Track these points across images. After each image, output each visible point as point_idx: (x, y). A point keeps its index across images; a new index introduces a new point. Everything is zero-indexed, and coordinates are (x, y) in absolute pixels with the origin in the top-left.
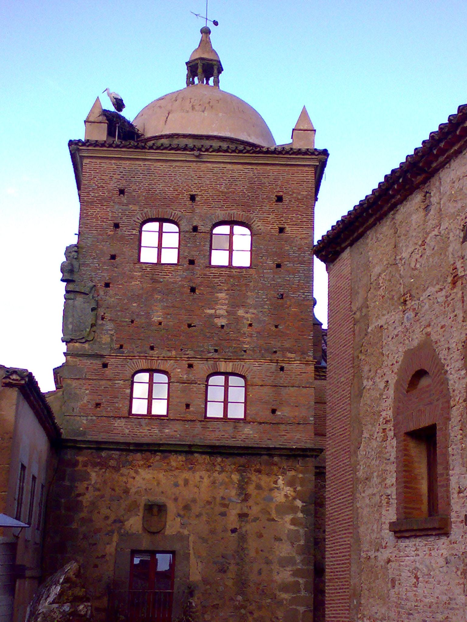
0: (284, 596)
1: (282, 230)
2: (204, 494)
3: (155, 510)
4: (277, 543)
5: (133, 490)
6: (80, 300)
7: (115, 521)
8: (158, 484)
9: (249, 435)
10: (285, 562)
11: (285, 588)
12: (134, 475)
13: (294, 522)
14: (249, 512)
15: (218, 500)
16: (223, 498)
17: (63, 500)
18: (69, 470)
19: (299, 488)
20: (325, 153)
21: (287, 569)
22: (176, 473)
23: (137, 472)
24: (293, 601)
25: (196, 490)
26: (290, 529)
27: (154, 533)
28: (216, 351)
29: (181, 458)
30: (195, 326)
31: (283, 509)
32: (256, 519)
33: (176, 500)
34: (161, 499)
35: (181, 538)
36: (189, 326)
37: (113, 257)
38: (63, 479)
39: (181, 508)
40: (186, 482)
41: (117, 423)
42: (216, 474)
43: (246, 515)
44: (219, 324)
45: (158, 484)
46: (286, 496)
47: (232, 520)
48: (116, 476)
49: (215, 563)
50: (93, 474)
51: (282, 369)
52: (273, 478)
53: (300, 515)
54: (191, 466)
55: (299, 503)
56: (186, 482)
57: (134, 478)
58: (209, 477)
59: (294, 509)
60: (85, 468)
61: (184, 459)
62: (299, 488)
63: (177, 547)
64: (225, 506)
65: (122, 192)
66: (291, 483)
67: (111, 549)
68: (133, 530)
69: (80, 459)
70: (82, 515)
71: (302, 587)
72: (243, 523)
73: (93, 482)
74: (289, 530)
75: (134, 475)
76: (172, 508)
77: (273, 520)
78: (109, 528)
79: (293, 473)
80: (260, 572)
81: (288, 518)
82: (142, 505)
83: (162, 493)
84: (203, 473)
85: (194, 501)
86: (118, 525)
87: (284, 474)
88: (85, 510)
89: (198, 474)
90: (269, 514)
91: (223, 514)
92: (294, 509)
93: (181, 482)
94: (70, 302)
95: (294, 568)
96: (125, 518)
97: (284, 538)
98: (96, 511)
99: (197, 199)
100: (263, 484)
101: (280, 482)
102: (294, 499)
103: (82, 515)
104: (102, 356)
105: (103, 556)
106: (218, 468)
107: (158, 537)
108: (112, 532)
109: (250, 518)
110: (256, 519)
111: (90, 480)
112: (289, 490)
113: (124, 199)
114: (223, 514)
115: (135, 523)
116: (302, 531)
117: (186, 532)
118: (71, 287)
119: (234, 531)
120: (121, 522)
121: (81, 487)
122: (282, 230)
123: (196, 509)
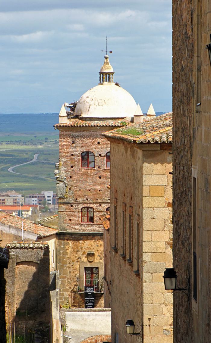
5: (84, 248)
7: (78, 258)
8: (92, 246)
17: (61, 252)
23: (85, 242)
29: (99, 237)
30: (101, 191)
33: (98, 251)
34: (92, 251)
36: (100, 191)
45: (92, 246)
50: (70, 243)
57: (83, 244)
60: (67, 241)
61: (100, 237)
75: (84, 243)
78: (77, 260)
93: (99, 245)
99: (100, 144)
105: (76, 269)
120: (80, 258)
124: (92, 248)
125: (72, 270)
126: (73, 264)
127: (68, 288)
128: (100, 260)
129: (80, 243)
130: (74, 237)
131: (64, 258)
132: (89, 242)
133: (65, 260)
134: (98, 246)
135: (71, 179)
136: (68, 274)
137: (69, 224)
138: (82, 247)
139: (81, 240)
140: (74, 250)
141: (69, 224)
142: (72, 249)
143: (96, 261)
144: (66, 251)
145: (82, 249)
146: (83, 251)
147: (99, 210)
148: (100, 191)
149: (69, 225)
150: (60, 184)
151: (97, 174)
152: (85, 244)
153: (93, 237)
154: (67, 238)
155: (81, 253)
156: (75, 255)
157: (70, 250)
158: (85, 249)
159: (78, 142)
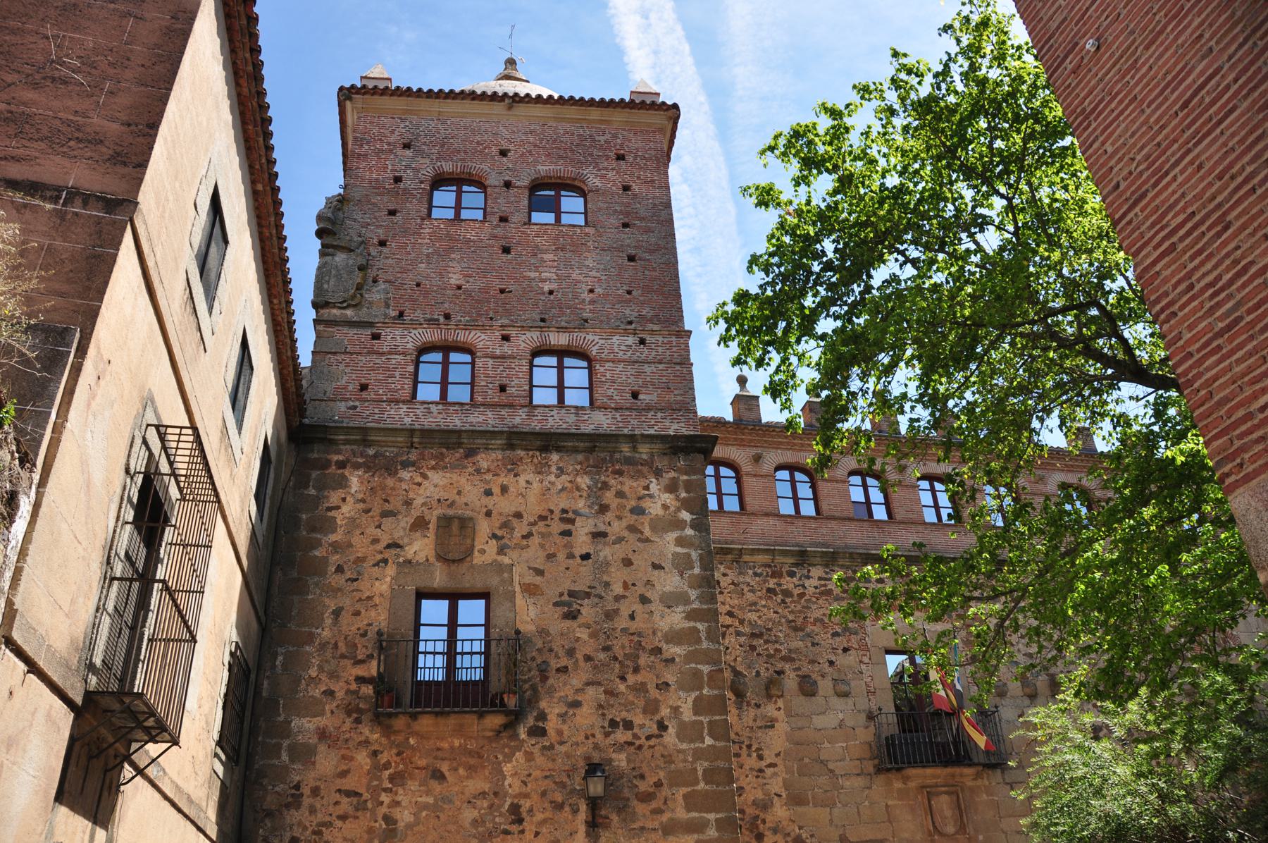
0: (676, 650)
1: (626, 188)
2: (533, 507)
3: (455, 527)
4: (656, 572)
5: (419, 501)
6: (340, 258)
7: (389, 546)
8: (459, 493)
9: (601, 422)
10: (670, 601)
11: (675, 637)
12: (419, 479)
13: (680, 542)
14: (608, 530)
15: (557, 512)
16: (564, 511)
17: (304, 516)
18: (315, 474)
19: (684, 495)
20: (675, 106)
21: (674, 609)
22: (489, 477)
23: (425, 477)
24: (689, 657)
25: (521, 500)
26: (678, 553)
27: (454, 561)
28: (543, 320)
31: (662, 526)
32: (620, 540)
33: (488, 514)
35: (499, 568)
36: (502, 291)
37: (392, 213)
38: (307, 487)
39: (497, 525)
40: (504, 489)
41: (392, 410)
42: (552, 478)
43: (603, 535)
44: (546, 289)
45: (459, 493)
46: (665, 507)
47: (582, 542)
48: (390, 482)
49: (556, 604)
51: (642, 342)
52: (644, 482)
53: (689, 532)
54: (513, 467)
55: (686, 516)
56: (504, 489)
57: (419, 484)
58: (541, 481)
59: (680, 525)
62: (684, 495)
63: (493, 582)
64: (572, 521)
65: (407, 146)
66: (672, 488)
67: (383, 587)
68: (421, 558)
69: (335, 458)
70: (333, 538)
71: (703, 635)
72: (600, 547)
73: (353, 491)
74: (675, 554)
75: (419, 479)
76: (484, 528)
77: (647, 540)
78: (379, 557)
79: (672, 474)
80: (632, 617)
81: (672, 536)
82: (434, 520)
83: (466, 504)
84: (531, 477)
85: (518, 515)
86: (394, 551)
87: (658, 473)
88: (340, 531)
89: (522, 480)
90: (642, 533)
91: (567, 533)
92: (680, 525)
94: (328, 258)
95: (688, 608)
96: (406, 540)
97: (667, 565)
98: (358, 532)
100: (626, 489)
101: (654, 488)
102: (678, 509)
103: (333, 538)
104: (371, 325)
105: (369, 598)
106: (554, 469)
107: (463, 567)
108: (385, 561)
109: (612, 538)
110: (620, 540)
111: (350, 487)
112: (667, 498)
113: (408, 153)
114: (567, 533)
115: (421, 548)
116: (695, 555)
117: (506, 560)
118: (329, 240)
119: (586, 557)
121: (334, 497)
122: (626, 188)
123: (521, 528)
124: (461, 501)
125: (346, 602)
126: (359, 573)
127: (317, 693)
128: (499, 558)
129: (401, 480)
130: (375, 456)
131: (317, 544)
132: (448, 475)
133: (317, 553)
134: (488, 493)
135: (385, 250)
136: (328, 621)
137: (357, 403)
138: (411, 495)
139: (405, 465)
140: (367, 511)
141: (357, 403)
142: (361, 506)
143: (478, 559)
144: (330, 514)
145: (408, 503)
146: (415, 513)
147: (498, 352)
148: (502, 291)
149: (355, 407)
150: (337, 259)
151: (495, 237)
152: (426, 483)
153: (467, 456)
154: (341, 458)
155: (406, 521)
156: (371, 531)
157: (345, 509)
158: (424, 504)
159: (424, 144)
